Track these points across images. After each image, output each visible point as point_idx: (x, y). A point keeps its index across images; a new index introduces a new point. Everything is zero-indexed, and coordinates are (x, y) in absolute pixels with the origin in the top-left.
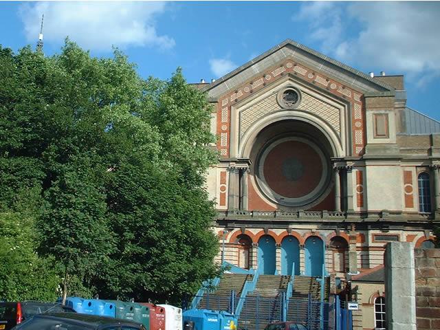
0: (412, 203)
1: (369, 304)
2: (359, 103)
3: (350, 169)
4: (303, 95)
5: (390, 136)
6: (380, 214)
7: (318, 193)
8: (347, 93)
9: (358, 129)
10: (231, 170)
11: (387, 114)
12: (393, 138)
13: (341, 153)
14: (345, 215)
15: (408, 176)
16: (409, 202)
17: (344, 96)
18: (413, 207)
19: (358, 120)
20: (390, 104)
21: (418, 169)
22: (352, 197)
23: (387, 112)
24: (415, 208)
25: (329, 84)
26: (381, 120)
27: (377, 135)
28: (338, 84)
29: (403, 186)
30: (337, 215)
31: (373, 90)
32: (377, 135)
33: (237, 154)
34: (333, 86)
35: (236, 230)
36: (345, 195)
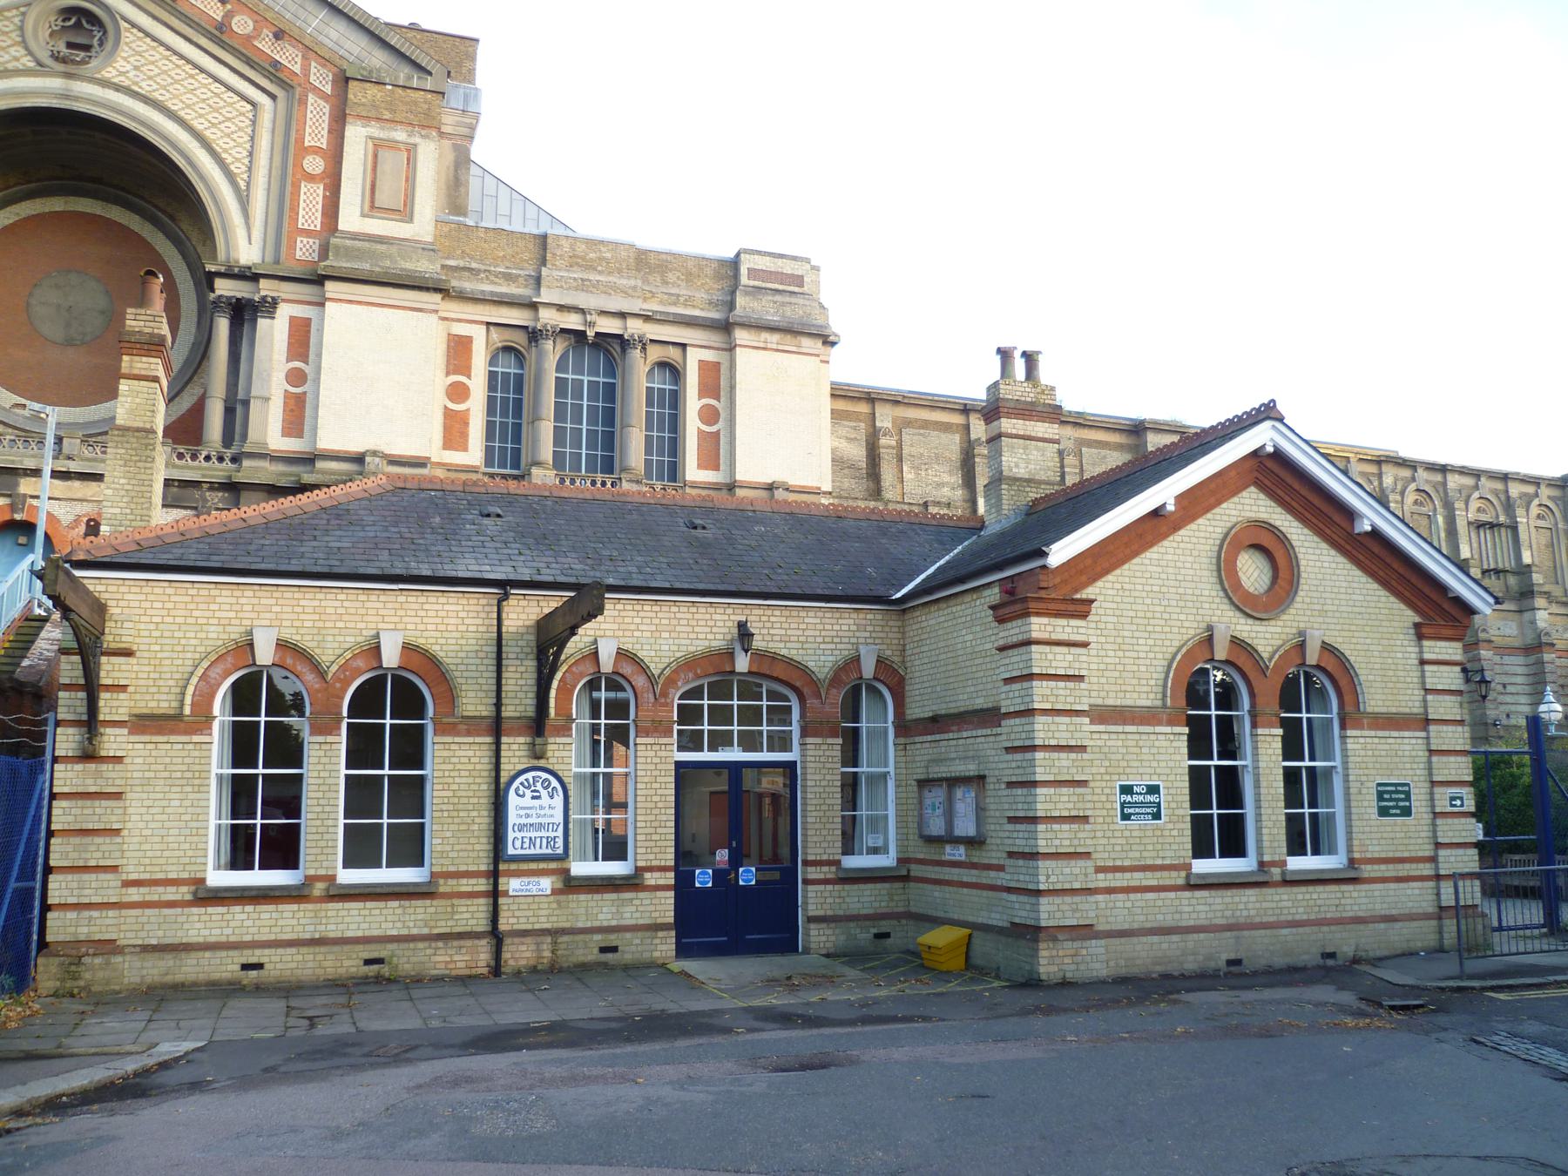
0: (464, 435)
1: (178, 717)
2: (325, 97)
3: (269, 307)
4: (128, 35)
5: (416, 216)
8: (289, 58)
9: (311, 178)
11: (411, 150)
12: (422, 226)
13: (243, 243)
14: (234, 460)
15: (458, 350)
17: (276, 64)
18: (465, 449)
19: (316, 150)
20: (427, 114)
21: (495, 334)
22: (267, 399)
23: (417, 140)
24: (473, 454)
25: (229, 15)
26: (391, 163)
27: (373, 208)
28: (260, 19)
29: (442, 381)
30: (208, 458)
31: (377, 59)
32: (373, 208)
34: (242, 24)
36: (241, 396)
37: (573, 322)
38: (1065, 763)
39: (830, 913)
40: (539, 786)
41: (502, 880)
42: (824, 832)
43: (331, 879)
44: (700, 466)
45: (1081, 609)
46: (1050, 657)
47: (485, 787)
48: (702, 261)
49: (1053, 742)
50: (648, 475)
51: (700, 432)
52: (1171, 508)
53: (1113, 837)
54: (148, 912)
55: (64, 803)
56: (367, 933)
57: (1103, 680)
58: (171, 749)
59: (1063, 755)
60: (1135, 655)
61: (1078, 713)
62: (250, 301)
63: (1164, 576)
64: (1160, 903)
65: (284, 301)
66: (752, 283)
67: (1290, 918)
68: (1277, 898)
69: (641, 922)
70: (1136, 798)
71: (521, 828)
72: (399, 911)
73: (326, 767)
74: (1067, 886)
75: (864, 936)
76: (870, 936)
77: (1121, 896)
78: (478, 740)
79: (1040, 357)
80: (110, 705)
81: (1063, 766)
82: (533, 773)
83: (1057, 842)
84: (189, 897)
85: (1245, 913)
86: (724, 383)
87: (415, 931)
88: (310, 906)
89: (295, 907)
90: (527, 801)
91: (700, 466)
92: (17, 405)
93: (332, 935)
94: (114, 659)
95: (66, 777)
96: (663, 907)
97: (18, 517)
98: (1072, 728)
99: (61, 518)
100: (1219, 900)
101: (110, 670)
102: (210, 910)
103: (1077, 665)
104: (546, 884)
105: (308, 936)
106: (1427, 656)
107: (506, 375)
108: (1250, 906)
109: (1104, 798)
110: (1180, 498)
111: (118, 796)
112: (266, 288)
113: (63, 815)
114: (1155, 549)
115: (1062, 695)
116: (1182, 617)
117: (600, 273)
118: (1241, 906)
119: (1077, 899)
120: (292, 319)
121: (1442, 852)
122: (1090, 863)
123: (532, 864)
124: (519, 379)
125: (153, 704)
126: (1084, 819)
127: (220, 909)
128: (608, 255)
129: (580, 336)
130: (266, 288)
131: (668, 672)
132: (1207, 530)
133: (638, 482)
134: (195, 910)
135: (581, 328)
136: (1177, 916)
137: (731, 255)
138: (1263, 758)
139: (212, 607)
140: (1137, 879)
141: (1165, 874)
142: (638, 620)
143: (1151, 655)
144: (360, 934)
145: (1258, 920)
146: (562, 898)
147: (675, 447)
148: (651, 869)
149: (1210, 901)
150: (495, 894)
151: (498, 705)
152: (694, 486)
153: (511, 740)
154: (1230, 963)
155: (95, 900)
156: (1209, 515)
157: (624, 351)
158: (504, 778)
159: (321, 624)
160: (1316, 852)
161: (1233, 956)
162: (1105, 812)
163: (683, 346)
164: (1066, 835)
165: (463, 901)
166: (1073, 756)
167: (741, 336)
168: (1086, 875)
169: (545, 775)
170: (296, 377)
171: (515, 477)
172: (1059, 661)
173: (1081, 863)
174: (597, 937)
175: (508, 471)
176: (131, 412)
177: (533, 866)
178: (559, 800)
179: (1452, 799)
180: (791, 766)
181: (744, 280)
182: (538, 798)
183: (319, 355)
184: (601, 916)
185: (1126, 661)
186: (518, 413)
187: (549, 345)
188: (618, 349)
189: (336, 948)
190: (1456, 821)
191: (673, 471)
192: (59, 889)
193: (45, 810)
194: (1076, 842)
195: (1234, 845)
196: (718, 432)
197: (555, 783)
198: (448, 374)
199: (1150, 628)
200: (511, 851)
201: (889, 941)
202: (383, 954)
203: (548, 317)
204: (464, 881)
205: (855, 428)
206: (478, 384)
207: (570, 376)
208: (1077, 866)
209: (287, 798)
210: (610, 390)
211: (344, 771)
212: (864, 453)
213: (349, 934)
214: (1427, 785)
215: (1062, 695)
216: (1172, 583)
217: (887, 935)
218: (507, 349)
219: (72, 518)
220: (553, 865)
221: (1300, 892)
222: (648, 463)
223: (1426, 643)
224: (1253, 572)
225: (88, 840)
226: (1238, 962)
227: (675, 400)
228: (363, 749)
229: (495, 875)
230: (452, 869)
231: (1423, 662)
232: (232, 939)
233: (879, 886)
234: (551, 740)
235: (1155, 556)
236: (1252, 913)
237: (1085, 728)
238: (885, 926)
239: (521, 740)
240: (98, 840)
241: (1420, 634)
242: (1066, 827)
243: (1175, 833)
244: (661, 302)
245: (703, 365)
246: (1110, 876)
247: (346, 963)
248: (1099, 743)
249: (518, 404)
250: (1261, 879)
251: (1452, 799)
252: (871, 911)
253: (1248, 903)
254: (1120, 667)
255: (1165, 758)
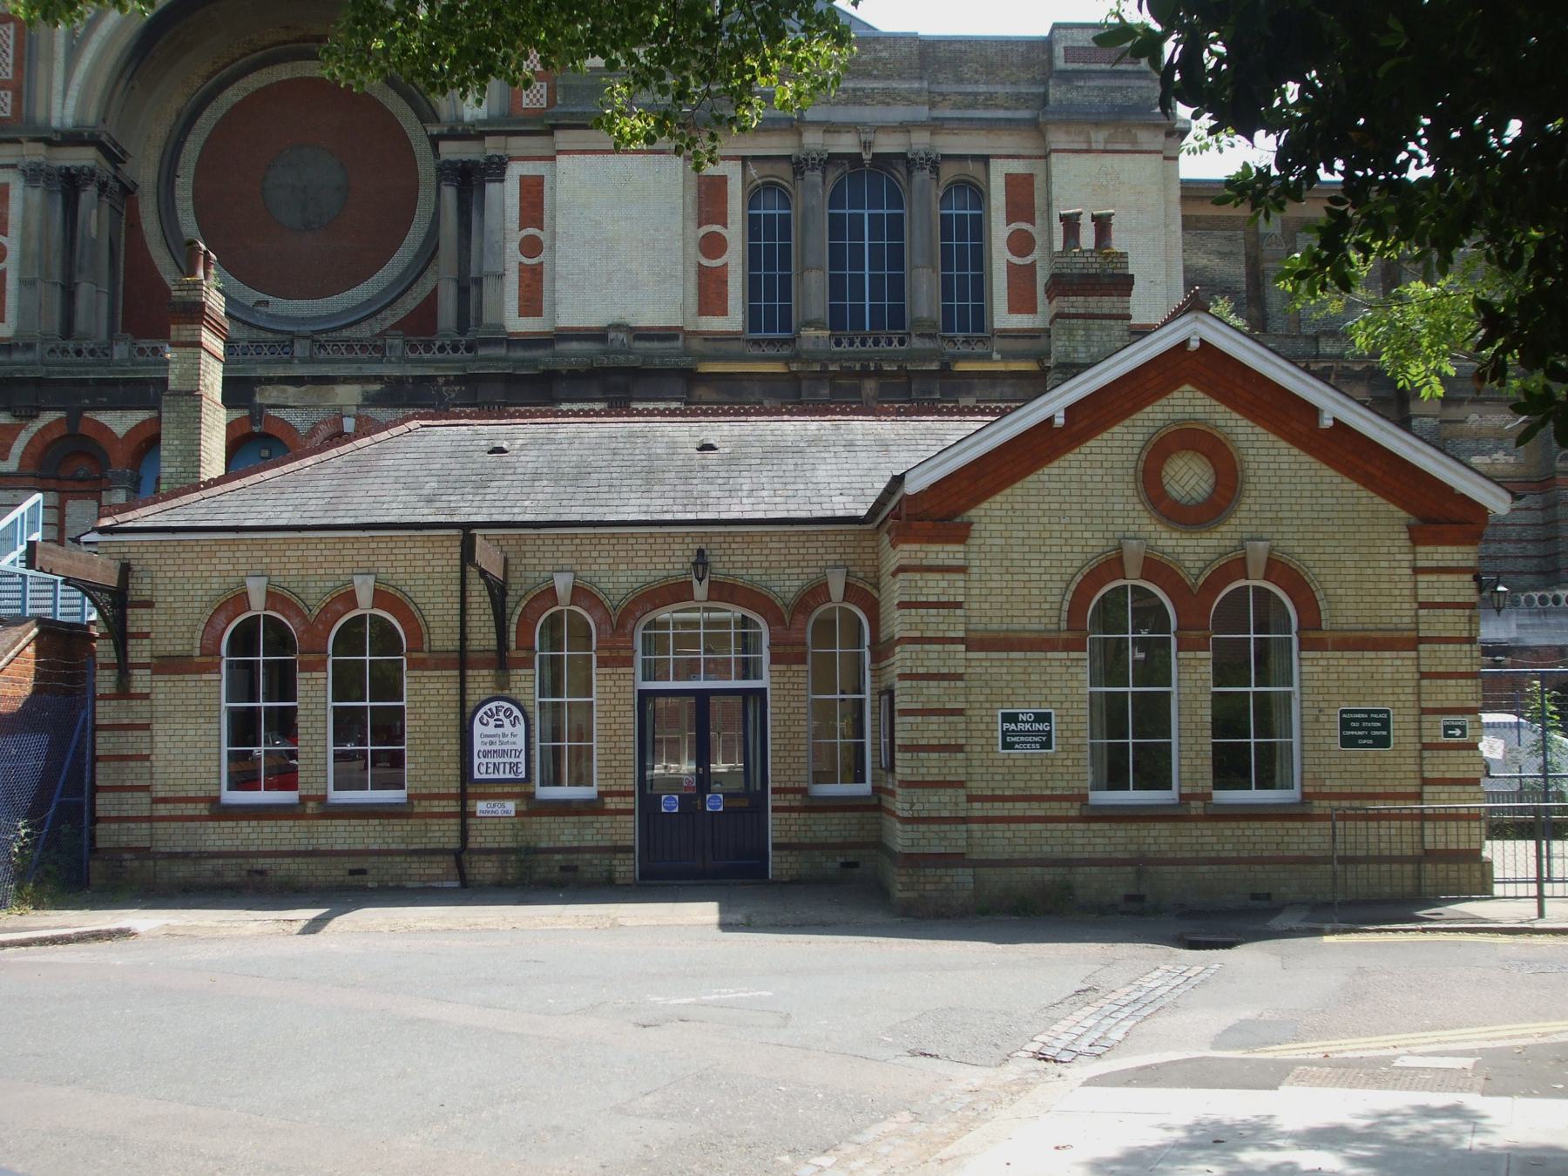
0: (723, 297)
3: (496, 168)
6: (599, 335)
7: (398, 280)
10: (33, 175)
16: (710, 292)
18: (724, 313)
21: (753, 171)
22: (501, 276)
24: (733, 320)
30: (442, 349)
33: (57, 101)
35: (48, 417)
36: (474, 274)
37: (846, 144)
38: (934, 691)
39: (794, 840)
40: (501, 715)
41: (470, 802)
42: (789, 760)
43: (322, 799)
44: (1013, 309)
45: (961, 534)
46: (920, 584)
47: (452, 716)
48: (1005, 46)
49: (921, 670)
50: (948, 326)
51: (1010, 266)
52: (1060, 421)
53: (996, 765)
54: (174, 825)
55: (105, 734)
56: (353, 847)
57: (987, 606)
58: (189, 685)
59: (933, 683)
60: (1025, 577)
61: (953, 641)
62: (475, 163)
63: (1064, 492)
64: (1048, 834)
65: (511, 159)
66: (1070, 66)
67: (1213, 854)
68: (1195, 833)
69: (601, 844)
70: (1021, 726)
71: (486, 754)
72: (379, 828)
73: (315, 697)
74: (934, 814)
75: (831, 865)
76: (837, 865)
77: (1000, 826)
78: (445, 673)
79: (1114, 220)
80: (139, 651)
81: (933, 693)
82: (496, 703)
83: (924, 771)
84: (206, 813)
85: (1153, 848)
86: (1039, 201)
87: (393, 847)
88: (303, 822)
89: (291, 823)
90: (491, 729)
91: (1013, 309)
92: (259, 303)
93: (323, 848)
94: (137, 611)
95: (106, 712)
96: (627, 830)
97: (256, 429)
98: (943, 655)
99: (299, 426)
100: (1122, 833)
101: (138, 620)
102: (223, 824)
103: (952, 591)
104: (510, 806)
105: (303, 848)
106: (1420, 564)
107: (770, 219)
108: (1162, 840)
109: (983, 727)
110: (1069, 410)
111: (147, 727)
112: (492, 146)
113: (105, 743)
114: (1056, 463)
115: (935, 624)
116: (1086, 535)
117: (876, 77)
118: (1151, 840)
119: (945, 827)
120: (523, 179)
121: (1427, 789)
122: (962, 792)
123: (495, 789)
124: (786, 220)
125: (170, 648)
126: (959, 748)
127: (230, 824)
128: (885, 54)
129: (855, 159)
130: (492, 146)
131: (624, 604)
132: (1122, 442)
133: (931, 336)
134: (211, 824)
135: (857, 150)
136: (1067, 848)
137: (1044, 31)
138: (1191, 684)
139: (215, 561)
140: (1020, 809)
141: (1055, 804)
142: (595, 554)
143: (1046, 577)
144: (346, 847)
145: (1171, 855)
146: (526, 819)
147: (980, 288)
148: (611, 794)
149: (1111, 834)
150: (465, 815)
151: (463, 638)
152: (1006, 334)
153: (475, 672)
154: (1129, 898)
155: (132, 813)
156: (1127, 422)
157: (910, 173)
158: (470, 705)
159: (303, 572)
160: (1266, 783)
161: (1133, 891)
162: (983, 741)
163: (985, 159)
164: (934, 763)
165: (435, 821)
166: (945, 684)
167: (1057, 138)
168: (956, 804)
169: (507, 705)
170: (531, 247)
171: (784, 342)
172: (934, 587)
173: (950, 791)
174: (558, 857)
175: (777, 335)
176: (179, 377)
177: (498, 790)
178: (520, 729)
179: (1447, 728)
180: (762, 692)
181: (1060, 64)
182: (501, 726)
183: (553, 218)
184: (563, 838)
185: (1016, 584)
186: (786, 265)
187: (815, 177)
188: (903, 170)
189: (327, 860)
190: (1453, 753)
191: (980, 317)
192: (105, 804)
193: (89, 739)
194: (946, 771)
195: (1154, 773)
196: (1033, 264)
197: (516, 712)
198: (700, 225)
199: (1044, 549)
200: (477, 776)
201: (857, 871)
202: (365, 866)
203: (813, 140)
204: (436, 803)
205: (1229, 239)
206: (734, 231)
207: (847, 211)
208: (946, 795)
209: (285, 724)
210: (897, 225)
211: (224, 704)
212: (1243, 270)
213: (338, 847)
214: (1415, 711)
215: (935, 624)
216: (1075, 499)
217: (855, 865)
218: (769, 187)
219: (309, 426)
220: (517, 789)
221: (1227, 829)
222: (947, 311)
223: (1421, 549)
224: (1188, 478)
225: (123, 764)
226: (1139, 898)
227: (979, 227)
228: (346, 684)
229: (463, 797)
230: (424, 791)
231: (1417, 571)
232: (241, 849)
233: (848, 815)
234: (513, 672)
235: (1056, 471)
236: (1163, 847)
237: (959, 655)
238: (852, 856)
239: (485, 672)
240: (132, 764)
241: (1417, 537)
242: (934, 755)
243: (1069, 763)
244: (955, 106)
245: (1010, 178)
246: (988, 805)
247: (334, 873)
248: (979, 670)
249: (786, 250)
250: (1179, 812)
251: (1453, 728)
252: (839, 840)
253: (1158, 838)
254: (1007, 592)
255: (1067, 687)
